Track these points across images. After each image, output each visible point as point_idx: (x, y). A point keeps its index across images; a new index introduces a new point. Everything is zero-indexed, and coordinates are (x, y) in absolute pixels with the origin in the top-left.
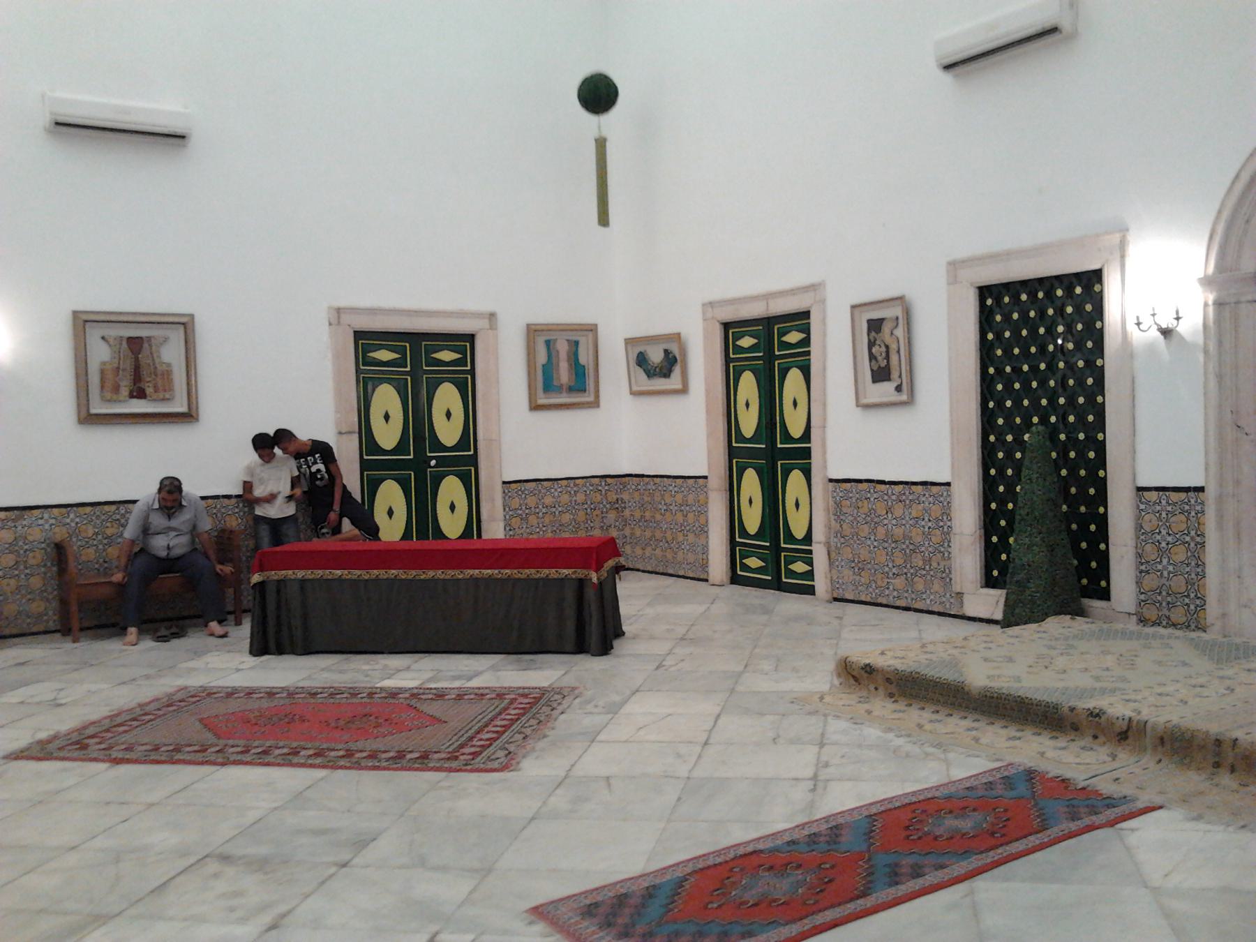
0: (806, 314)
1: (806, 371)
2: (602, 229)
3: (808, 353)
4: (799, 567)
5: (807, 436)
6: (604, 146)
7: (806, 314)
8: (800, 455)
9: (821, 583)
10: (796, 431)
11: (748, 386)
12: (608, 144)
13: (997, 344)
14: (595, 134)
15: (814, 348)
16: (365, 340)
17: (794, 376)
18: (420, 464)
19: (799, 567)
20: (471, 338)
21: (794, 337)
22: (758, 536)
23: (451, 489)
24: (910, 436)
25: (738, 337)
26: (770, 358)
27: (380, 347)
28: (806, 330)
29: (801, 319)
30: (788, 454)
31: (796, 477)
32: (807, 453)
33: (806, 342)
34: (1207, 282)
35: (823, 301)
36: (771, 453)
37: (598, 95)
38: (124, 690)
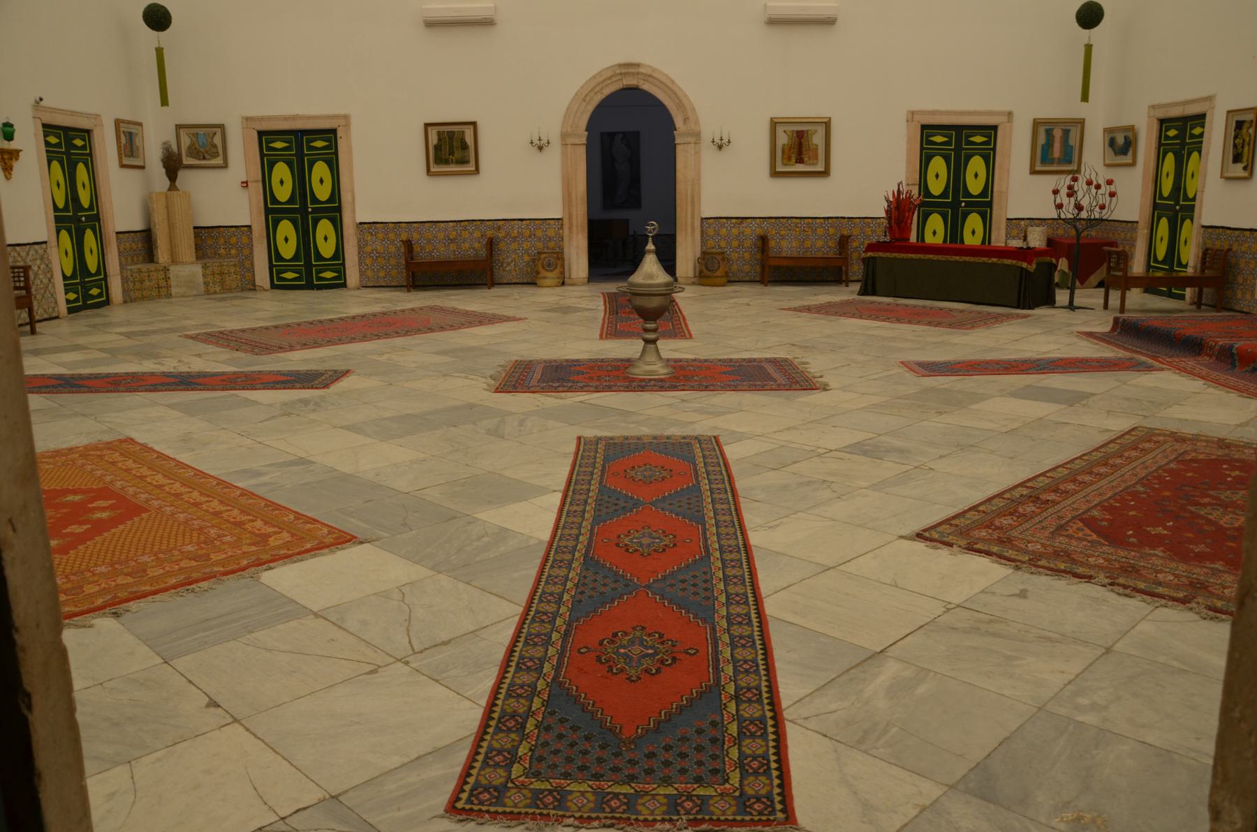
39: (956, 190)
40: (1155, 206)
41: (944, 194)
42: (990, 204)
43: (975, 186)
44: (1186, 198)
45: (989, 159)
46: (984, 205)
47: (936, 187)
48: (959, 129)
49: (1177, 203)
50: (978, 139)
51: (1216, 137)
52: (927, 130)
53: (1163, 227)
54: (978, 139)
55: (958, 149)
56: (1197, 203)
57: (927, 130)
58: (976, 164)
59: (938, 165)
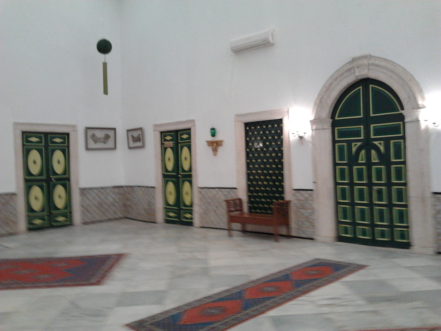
0: (190, 129)
1: (189, 148)
2: (105, 95)
3: (190, 142)
4: (188, 216)
5: (190, 170)
6: (106, 67)
7: (190, 129)
8: (188, 177)
9: (197, 221)
10: (186, 168)
11: (170, 153)
12: (108, 65)
13: (250, 141)
14: (103, 61)
15: (192, 140)
16: (26, 135)
17: (185, 149)
18: (48, 180)
19: (188, 216)
20: (68, 134)
21: (185, 136)
22: (174, 206)
23: (59, 190)
24: (221, 170)
25: (165, 136)
26: (177, 143)
27: (31, 137)
28: (189, 134)
29: (188, 131)
30: (184, 176)
31: (187, 184)
32: (190, 176)
33: (189, 138)
34: (312, 122)
35: (194, 126)
36: (178, 175)
37: (104, 47)
38: (266, 304)
39: (48, 171)
40: (164, 176)
41: (41, 174)
42: (68, 179)
43: (59, 169)
44: (184, 171)
45: (66, 152)
46: (65, 180)
47: (35, 169)
48: (46, 134)
49: (178, 173)
50: (58, 140)
51: (200, 138)
52: (26, 135)
53: (171, 187)
54: (58, 140)
55: (46, 146)
56: (193, 173)
57: (26, 135)
58: (58, 155)
59: (35, 155)
